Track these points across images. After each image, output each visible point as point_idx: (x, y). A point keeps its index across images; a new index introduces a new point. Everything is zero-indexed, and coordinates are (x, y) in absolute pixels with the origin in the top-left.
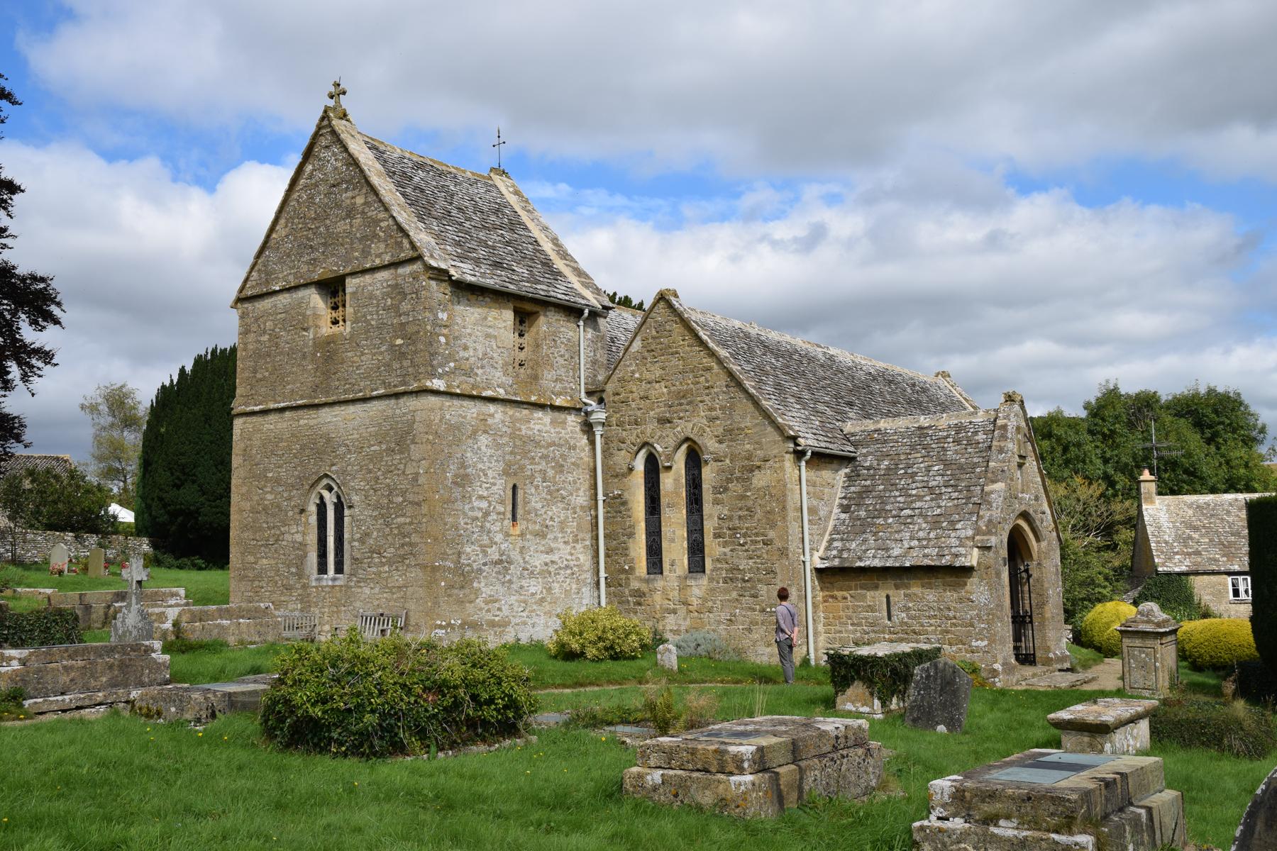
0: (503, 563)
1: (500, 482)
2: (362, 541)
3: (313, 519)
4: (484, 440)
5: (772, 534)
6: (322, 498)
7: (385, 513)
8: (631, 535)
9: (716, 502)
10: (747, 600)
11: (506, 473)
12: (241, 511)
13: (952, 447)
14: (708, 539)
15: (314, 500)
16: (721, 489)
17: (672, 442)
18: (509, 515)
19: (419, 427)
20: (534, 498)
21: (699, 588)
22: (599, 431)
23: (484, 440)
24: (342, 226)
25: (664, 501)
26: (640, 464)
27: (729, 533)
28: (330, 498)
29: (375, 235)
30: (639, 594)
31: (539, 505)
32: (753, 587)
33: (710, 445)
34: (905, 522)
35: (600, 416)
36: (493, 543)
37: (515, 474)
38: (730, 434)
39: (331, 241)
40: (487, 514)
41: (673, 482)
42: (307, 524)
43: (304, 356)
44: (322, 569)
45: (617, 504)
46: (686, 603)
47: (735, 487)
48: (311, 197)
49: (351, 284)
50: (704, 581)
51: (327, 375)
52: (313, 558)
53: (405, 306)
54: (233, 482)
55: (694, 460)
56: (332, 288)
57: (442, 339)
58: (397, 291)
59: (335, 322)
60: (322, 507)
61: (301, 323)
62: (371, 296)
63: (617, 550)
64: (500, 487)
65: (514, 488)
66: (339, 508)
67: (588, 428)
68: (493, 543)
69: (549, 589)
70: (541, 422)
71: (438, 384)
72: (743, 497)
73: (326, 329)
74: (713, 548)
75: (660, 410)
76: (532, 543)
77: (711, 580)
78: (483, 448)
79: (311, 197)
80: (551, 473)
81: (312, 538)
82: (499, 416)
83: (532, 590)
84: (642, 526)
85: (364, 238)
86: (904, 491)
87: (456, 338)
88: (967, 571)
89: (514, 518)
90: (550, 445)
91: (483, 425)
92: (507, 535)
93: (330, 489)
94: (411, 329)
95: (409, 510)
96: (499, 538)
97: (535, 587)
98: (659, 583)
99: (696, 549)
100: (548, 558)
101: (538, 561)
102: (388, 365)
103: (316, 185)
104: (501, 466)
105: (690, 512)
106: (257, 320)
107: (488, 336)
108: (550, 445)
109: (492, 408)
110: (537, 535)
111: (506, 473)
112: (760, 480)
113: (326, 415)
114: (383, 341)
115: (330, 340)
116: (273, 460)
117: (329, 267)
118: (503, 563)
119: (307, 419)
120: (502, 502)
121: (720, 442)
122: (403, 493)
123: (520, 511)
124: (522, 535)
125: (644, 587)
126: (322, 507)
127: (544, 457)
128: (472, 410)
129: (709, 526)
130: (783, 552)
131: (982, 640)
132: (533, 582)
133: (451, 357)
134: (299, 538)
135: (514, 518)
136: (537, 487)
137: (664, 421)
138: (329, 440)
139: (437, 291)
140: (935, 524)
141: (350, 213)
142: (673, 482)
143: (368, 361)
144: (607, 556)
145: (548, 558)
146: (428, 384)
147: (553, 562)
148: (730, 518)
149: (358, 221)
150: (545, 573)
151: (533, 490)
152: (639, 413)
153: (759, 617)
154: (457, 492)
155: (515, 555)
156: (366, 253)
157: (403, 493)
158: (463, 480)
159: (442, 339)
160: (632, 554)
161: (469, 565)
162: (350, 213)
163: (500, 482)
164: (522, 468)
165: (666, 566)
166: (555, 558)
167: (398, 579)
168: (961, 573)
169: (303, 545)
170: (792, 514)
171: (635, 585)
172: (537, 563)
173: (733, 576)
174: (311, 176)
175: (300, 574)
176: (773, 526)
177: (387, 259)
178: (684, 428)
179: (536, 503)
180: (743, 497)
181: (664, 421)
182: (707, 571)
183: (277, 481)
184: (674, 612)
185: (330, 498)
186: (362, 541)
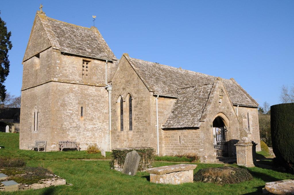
0: (77, 128)
1: (77, 106)
4: (71, 95)
5: (147, 119)
8: (117, 120)
9: (135, 110)
10: (141, 138)
11: (79, 103)
13: (202, 94)
16: (136, 107)
17: (125, 94)
18: (80, 115)
19: (51, 91)
20: (88, 110)
22: (110, 92)
23: (71, 95)
26: (119, 101)
28: (36, 111)
30: (118, 136)
31: (90, 112)
32: (143, 134)
33: (134, 95)
35: (110, 88)
36: (74, 122)
37: (82, 104)
40: (72, 114)
41: (126, 105)
46: (128, 138)
47: (139, 106)
51: (36, 78)
53: (49, 60)
55: (130, 100)
57: (58, 68)
64: (77, 107)
65: (82, 108)
68: (74, 122)
69: (94, 135)
70: (92, 90)
71: (55, 79)
72: (140, 109)
75: (123, 86)
76: (88, 123)
77: (134, 132)
78: (71, 97)
80: (95, 103)
81: (33, 121)
82: (77, 88)
83: (88, 135)
84: (120, 117)
85: (43, 43)
87: (63, 67)
89: (82, 115)
90: (94, 96)
91: (71, 91)
92: (79, 120)
96: (76, 121)
97: (89, 134)
98: (122, 133)
99: (131, 124)
100: (93, 126)
101: (90, 127)
104: (77, 102)
107: (73, 67)
108: (94, 96)
109: (74, 86)
110: (90, 120)
111: (79, 103)
118: (77, 128)
120: (77, 111)
121: (136, 94)
123: (83, 114)
124: (84, 120)
127: (93, 99)
128: (67, 86)
130: (149, 124)
131: (202, 148)
132: (88, 132)
133: (61, 72)
135: (82, 115)
136: (90, 108)
137: (124, 89)
139: (56, 54)
144: (112, 126)
145: (93, 126)
146: (52, 79)
147: (95, 128)
148: (138, 115)
150: (93, 130)
151: (88, 108)
152: (119, 87)
154: (61, 108)
155: (82, 125)
158: (64, 105)
159: (58, 68)
160: (117, 125)
161: (65, 128)
163: (77, 106)
164: (85, 102)
166: (96, 126)
170: (152, 113)
171: (118, 134)
172: (89, 127)
175: (31, 131)
178: (128, 90)
179: (89, 111)
182: (133, 130)
184: (126, 141)
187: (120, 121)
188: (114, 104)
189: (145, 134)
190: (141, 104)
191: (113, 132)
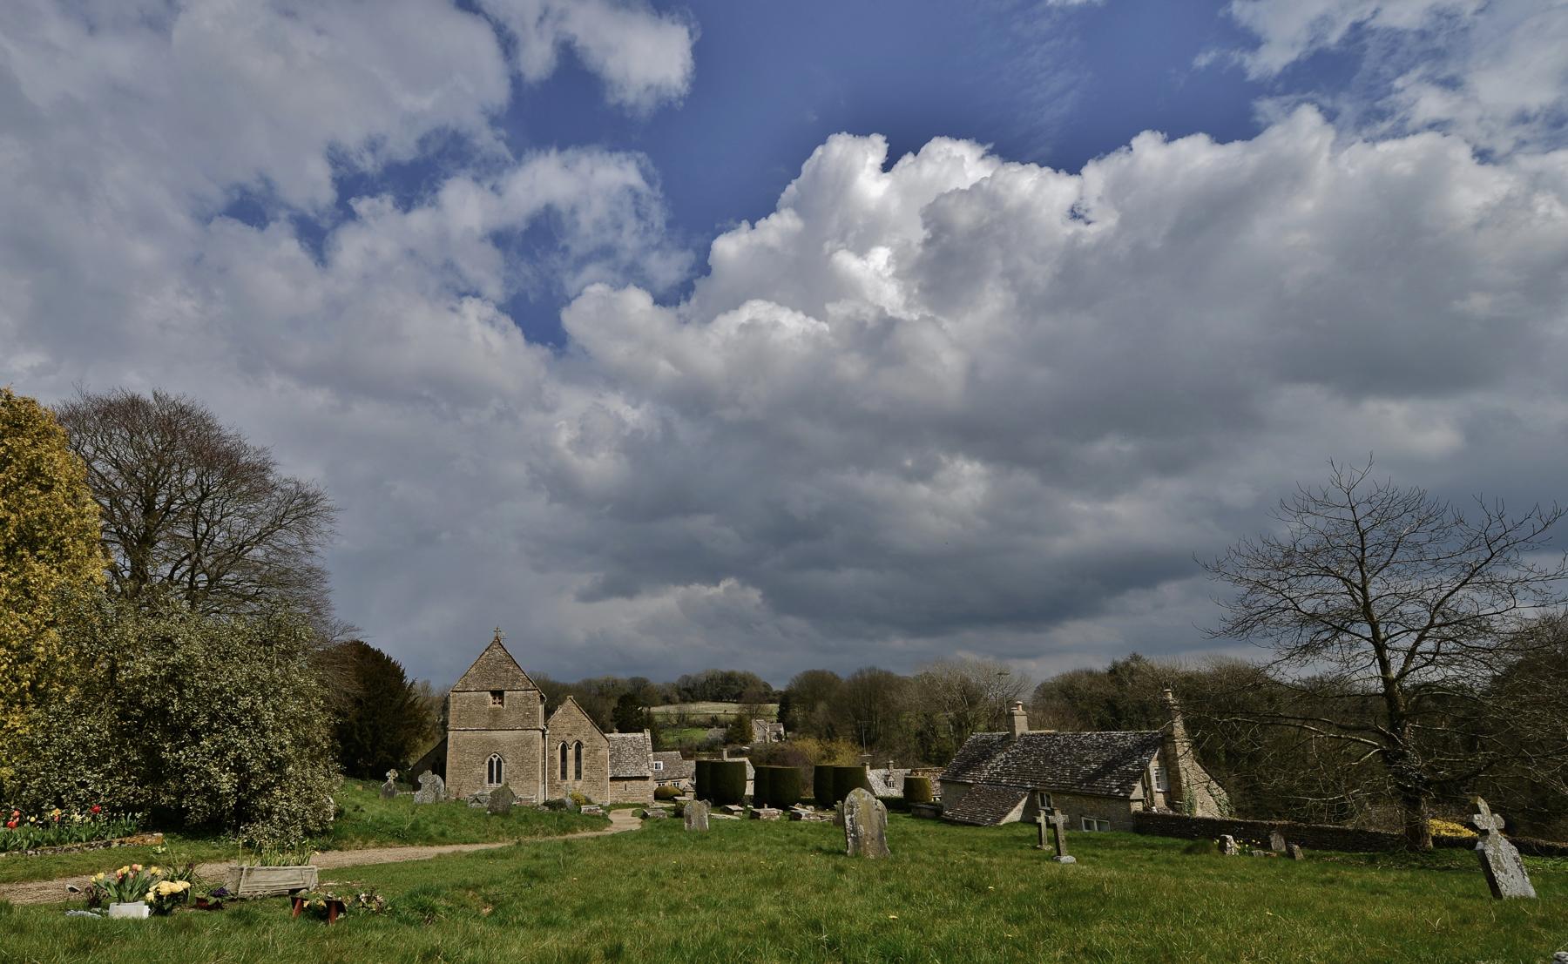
7: (521, 764)
21: (579, 784)
38: (591, 740)
41: (571, 753)
44: (491, 781)
45: (552, 759)
49: (506, 694)
55: (579, 745)
56: (498, 694)
60: (491, 762)
61: (484, 703)
63: (552, 772)
66: (499, 762)
74: (584, 772)
113: (495, 734)
117: (496, 687)
119: (485, 734)
126: (491, 762)
142: (571, 753)
168: (646, 778)
188: (551, 750)
191: (552, 781)
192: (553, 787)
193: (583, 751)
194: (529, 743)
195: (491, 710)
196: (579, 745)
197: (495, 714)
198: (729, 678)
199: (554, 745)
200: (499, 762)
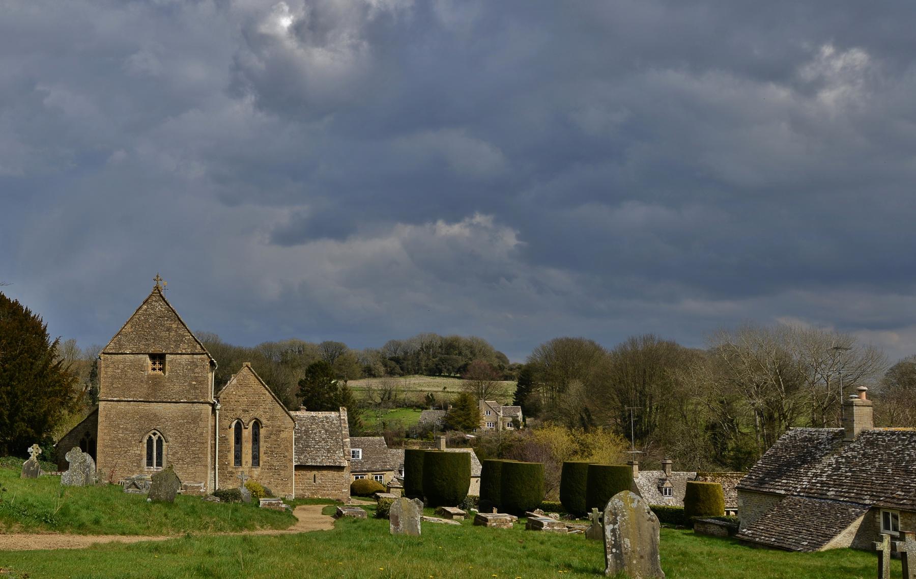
2: (173, 455)
3: (145, 445)
6: (150, 437)
9: (265, 442)
12: (104, 440)
14: (261, 454)
15: (147, 437)
17: (248, 420)
21: (256, 472)
22: (217, 412)
24: (163, 334)
25: (244, 440)
27: (270, 452)
28: (155, 438)
29: (182, 340)
30: (231, 473)
33: (264, 421)
34: (318, 450)
38: (272, 418)
39: (157, 339)
41: (247, 433)
42: (143, 447)
43: (142, 382)
44: (150, 463)
45: (224, 440)
48: (146, 320)
49: (169, 358)
50: (259, 469)
52: (145, 460)
53: (197, 370)
54: (99, 427)
55: (257, 424)
56: (158, 358)
58: (194, 364)
59: (154, 369)
60: (150, 441)
61: (142, 368)
62: (180, 364)
63: (223, 456)
66: (159, 441)
67: (214, 410)
72: (276, 441)
73: (151, 372)
74: (263, 458)
75: (244, 407)
79: (146, 320)
81: (145, 453)
86: (314, 439)
88: (344, 467)
93: (155, 434)
94: (200, 379)
95: (198, 445)
98: (241, 469)
102: (188, 391)
103: (149, 315)
105: (253, 444)
106: (113, 363)
112: (283, 435)
113: (154, 406)
114: (185, 381)
115: (154, 378)
116: (124, 420)
119: (142, 406)
122: (195, 439)
125: (234, 471)
126: (150, 441)
129: (262, 450)
134: (138, 452)
137: (244, 411)
138: (156, 416)
140: (329, 451)
141: (169, 329)
142: (247, 433)
143: (177, 388)
149: (173, 333)
153: (281, 482)
156: (177, 346)
157: (195, 439)
162: (169, 329)
165: (244, 463)
167: (192, 470)
168: (340, 468)
169: (140, 455)
171: (230, 470)
173: (271, 467)
174: (146, 310)
175: (139, 466)
176: (287, 451)
177: (189, 351)
180: (276, 441)
181: (244, 411)
183: (126, 429)
185: (155, 438)
186: (173, 455)
187: (233, 452)
188: (222, 429)
189: (282, 473)
190: (277, 435)
191: (223, 466)
192: (225, 475)
193: (263, 432)
194: (195, 419)
195: (149, 377)
196: (257, 424)
197: (155, 383)
198: (450, 346)
199: (226, 423)
200: (159, 441)
